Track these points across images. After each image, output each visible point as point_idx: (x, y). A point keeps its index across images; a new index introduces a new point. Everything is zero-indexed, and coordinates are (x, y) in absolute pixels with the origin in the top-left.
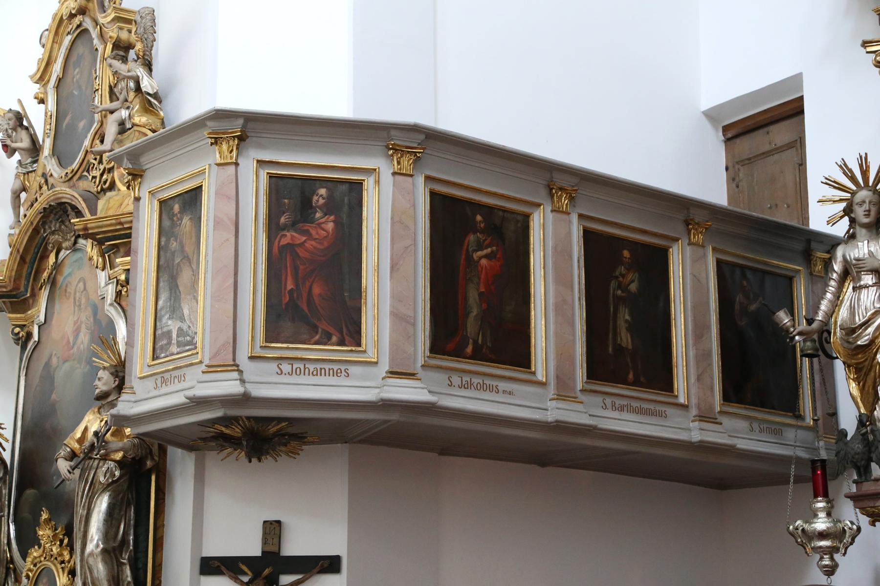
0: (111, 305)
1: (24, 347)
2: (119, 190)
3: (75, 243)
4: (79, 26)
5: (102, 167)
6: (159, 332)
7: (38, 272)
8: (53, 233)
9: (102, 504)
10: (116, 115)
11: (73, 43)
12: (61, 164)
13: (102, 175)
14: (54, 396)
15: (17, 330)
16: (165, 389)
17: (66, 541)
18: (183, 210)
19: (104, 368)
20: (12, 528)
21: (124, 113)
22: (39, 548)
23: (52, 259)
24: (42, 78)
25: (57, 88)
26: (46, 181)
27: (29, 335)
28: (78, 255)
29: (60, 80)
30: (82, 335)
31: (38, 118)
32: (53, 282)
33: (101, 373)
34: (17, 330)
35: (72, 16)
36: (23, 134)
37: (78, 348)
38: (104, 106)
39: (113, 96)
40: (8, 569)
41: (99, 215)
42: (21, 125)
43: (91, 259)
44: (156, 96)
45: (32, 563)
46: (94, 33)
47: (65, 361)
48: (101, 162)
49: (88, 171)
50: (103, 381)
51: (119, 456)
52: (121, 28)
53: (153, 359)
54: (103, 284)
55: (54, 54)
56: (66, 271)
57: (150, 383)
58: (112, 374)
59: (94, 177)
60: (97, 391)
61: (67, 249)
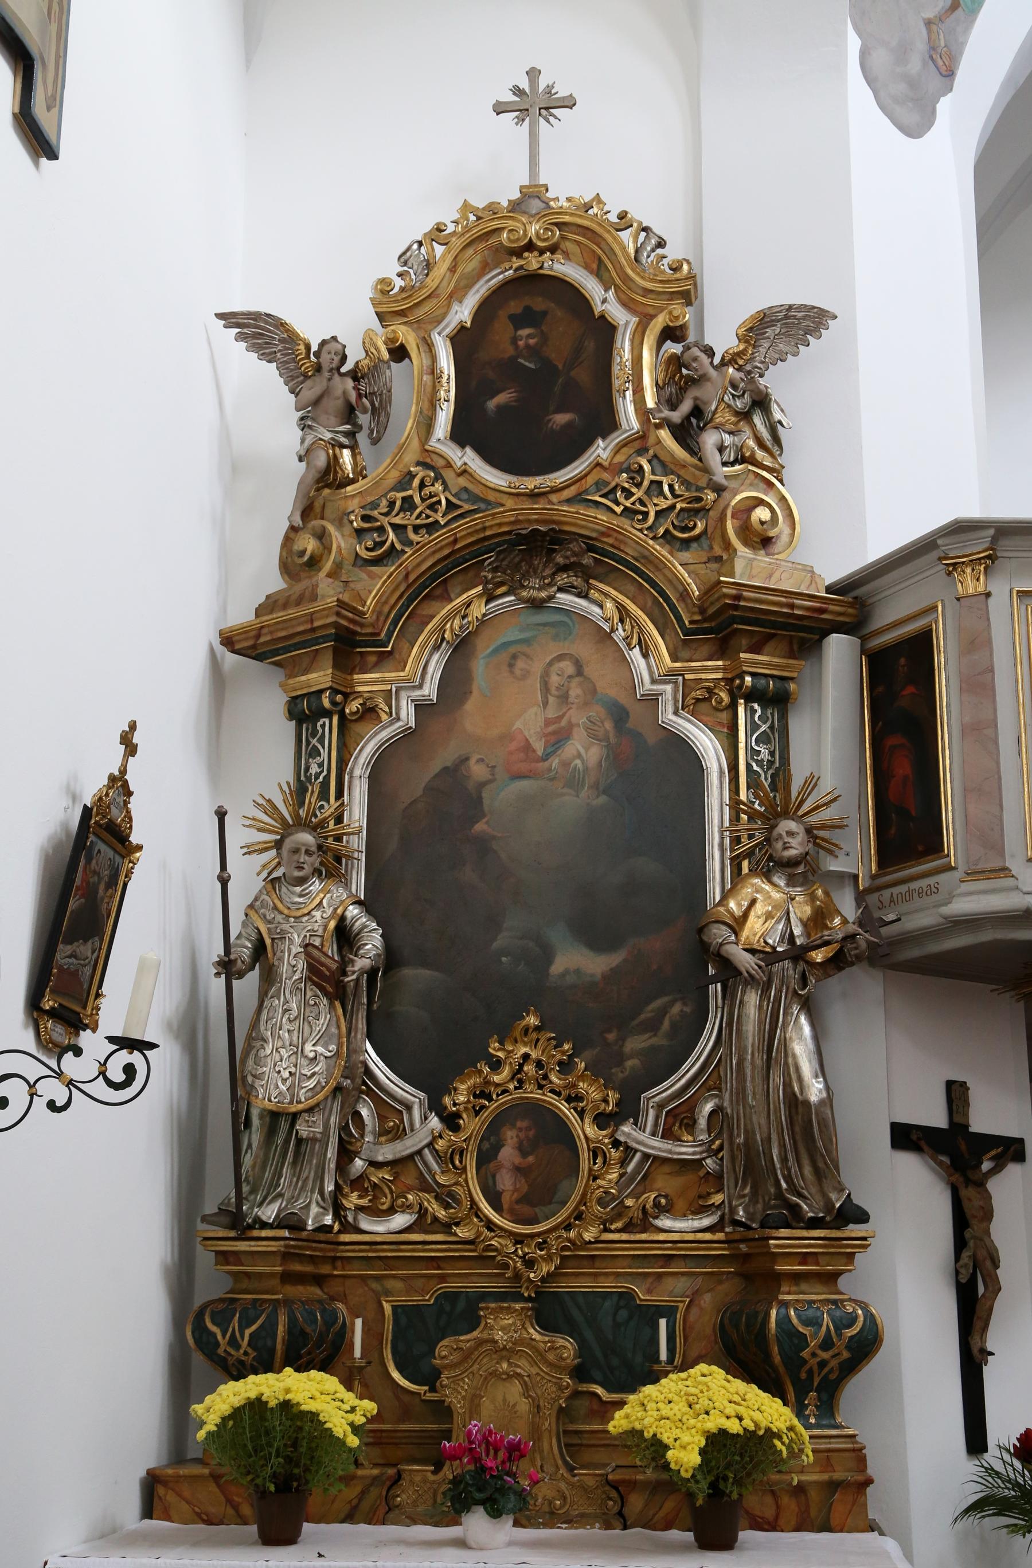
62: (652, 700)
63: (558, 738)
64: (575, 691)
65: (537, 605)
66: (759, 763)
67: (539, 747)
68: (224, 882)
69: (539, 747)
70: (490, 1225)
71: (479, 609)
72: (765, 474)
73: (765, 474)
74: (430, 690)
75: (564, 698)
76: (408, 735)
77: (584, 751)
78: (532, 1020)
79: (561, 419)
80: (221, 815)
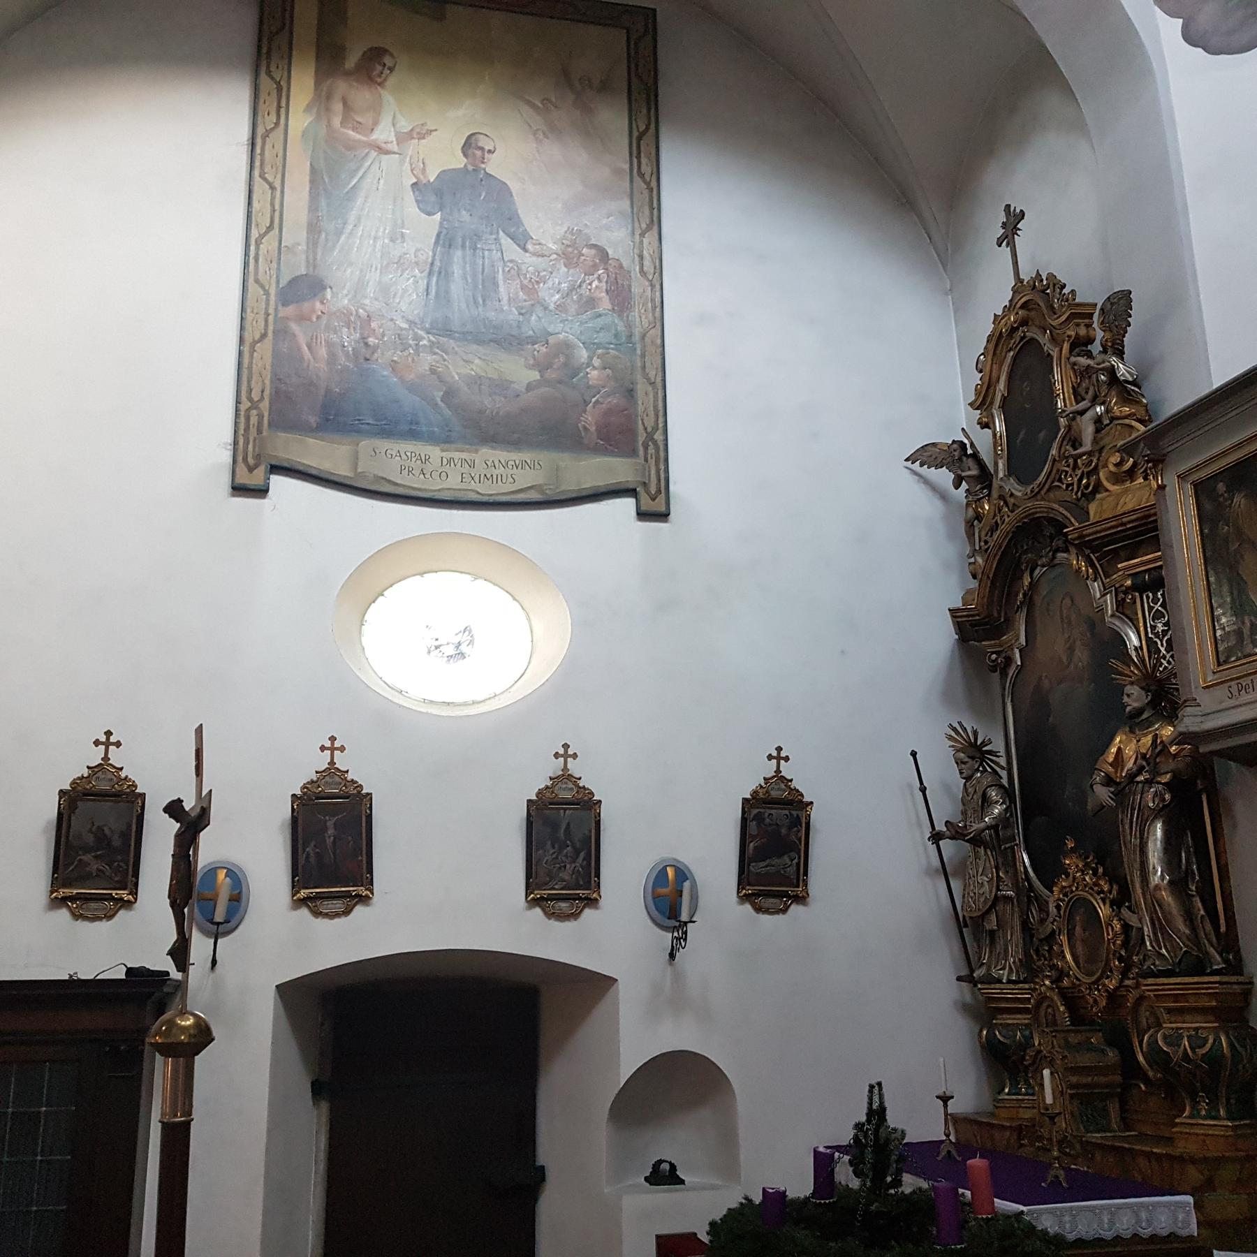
0: (1112, 616)
1: (1004, 674)
2: (1107, 490)
3: (1054, 557)
4: (1022, 338)
5: (1079, 472)
6: (1219, 633)
7: (1011, 595)
8: (1026, 552)
9: (1159, 830)
10: (1089, 414)
11: (1015, 358)
12: (1020, 481)
13: (1080, 480)
14: (1051, 719)
15: (994, 656)
16: (1245, 698)
17: (1101, 870)
18: (1231, 490)
19: (1132, 683)
20: (1025, 856)
21: (1099, 409)
22: (1067, 875)
23: (1027, 581)
24: (982, 401)
25: (1003, 407)
26: (1006, 503)
27: (1009, 660)
28: (1058, 570)
29: (1004, 399)
30: (1078, 653)
31: (983, 442)
32: (1029, 602)
33: (1128, 689)
34: (994, 656)
35: (1013, 330)
36: (970, 462)
37: (1076, 667)
38: (1070, 409)
39: (1078, 398)
40: (1029, 897)
41: (1092, 520)
42: (966, 454)
43: (1078, 571)
44: (1134, 383)
45: (1061, 891)
46: (1044, 340)
47: (1060, 683)
48: (1075, 467)
49: (1060, 480)
50: (1134, 697)
51: (1166, 778)
52: (1078, 325)
53: (1219, 665)
54: (1098, 595)
55: (994, 375)
56: (1044, 590)
57: (1221, 692)
58: (1142, 688)
59: (1068, 486)
60: (1128, 709)
61: (1043, 566)
62: (1102, 611)
63: (1071, 649)
64: (1073, 617)
65: (1052, 565)
66: (1157, 635)
67: (1064, 659)
68: (923, 790)
69: (1064, 659)
70: (1078, 979)
71: (1027, 581)
72: (1127, 421)
73: (1127, 421)
74: (1023, 640)
75: (1069, 623)
76: (1020, 669)
77: (1082, 656)
78: (1070, 844)
79: (1042, 435)
80: (914, 754)
